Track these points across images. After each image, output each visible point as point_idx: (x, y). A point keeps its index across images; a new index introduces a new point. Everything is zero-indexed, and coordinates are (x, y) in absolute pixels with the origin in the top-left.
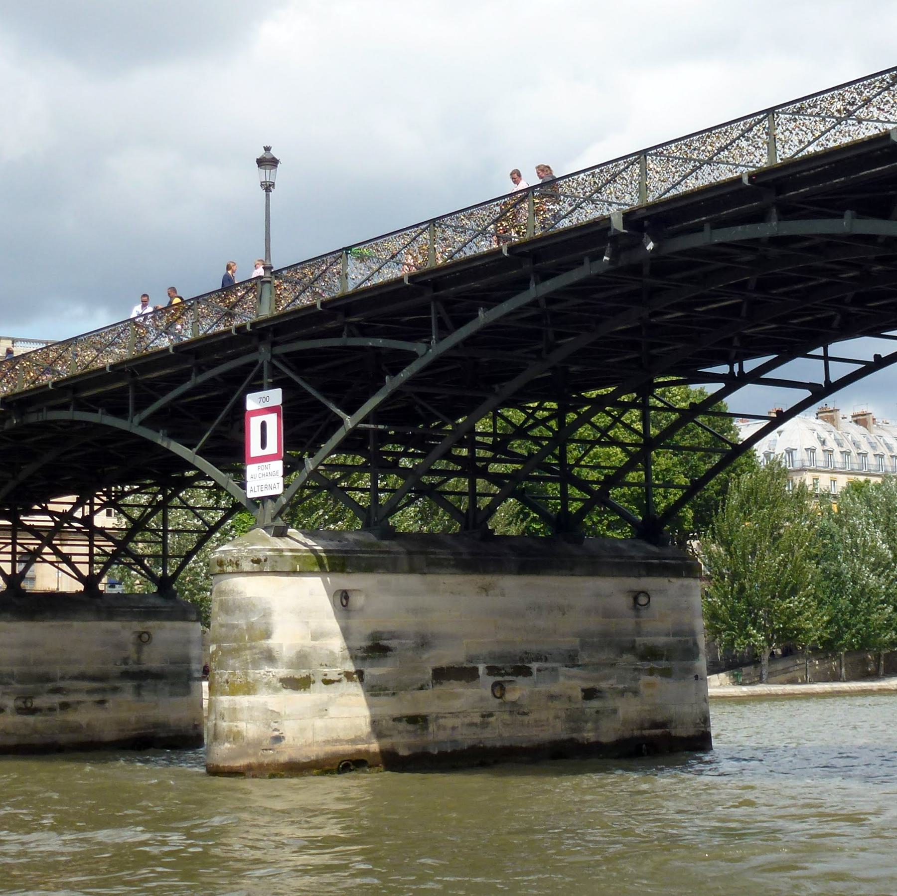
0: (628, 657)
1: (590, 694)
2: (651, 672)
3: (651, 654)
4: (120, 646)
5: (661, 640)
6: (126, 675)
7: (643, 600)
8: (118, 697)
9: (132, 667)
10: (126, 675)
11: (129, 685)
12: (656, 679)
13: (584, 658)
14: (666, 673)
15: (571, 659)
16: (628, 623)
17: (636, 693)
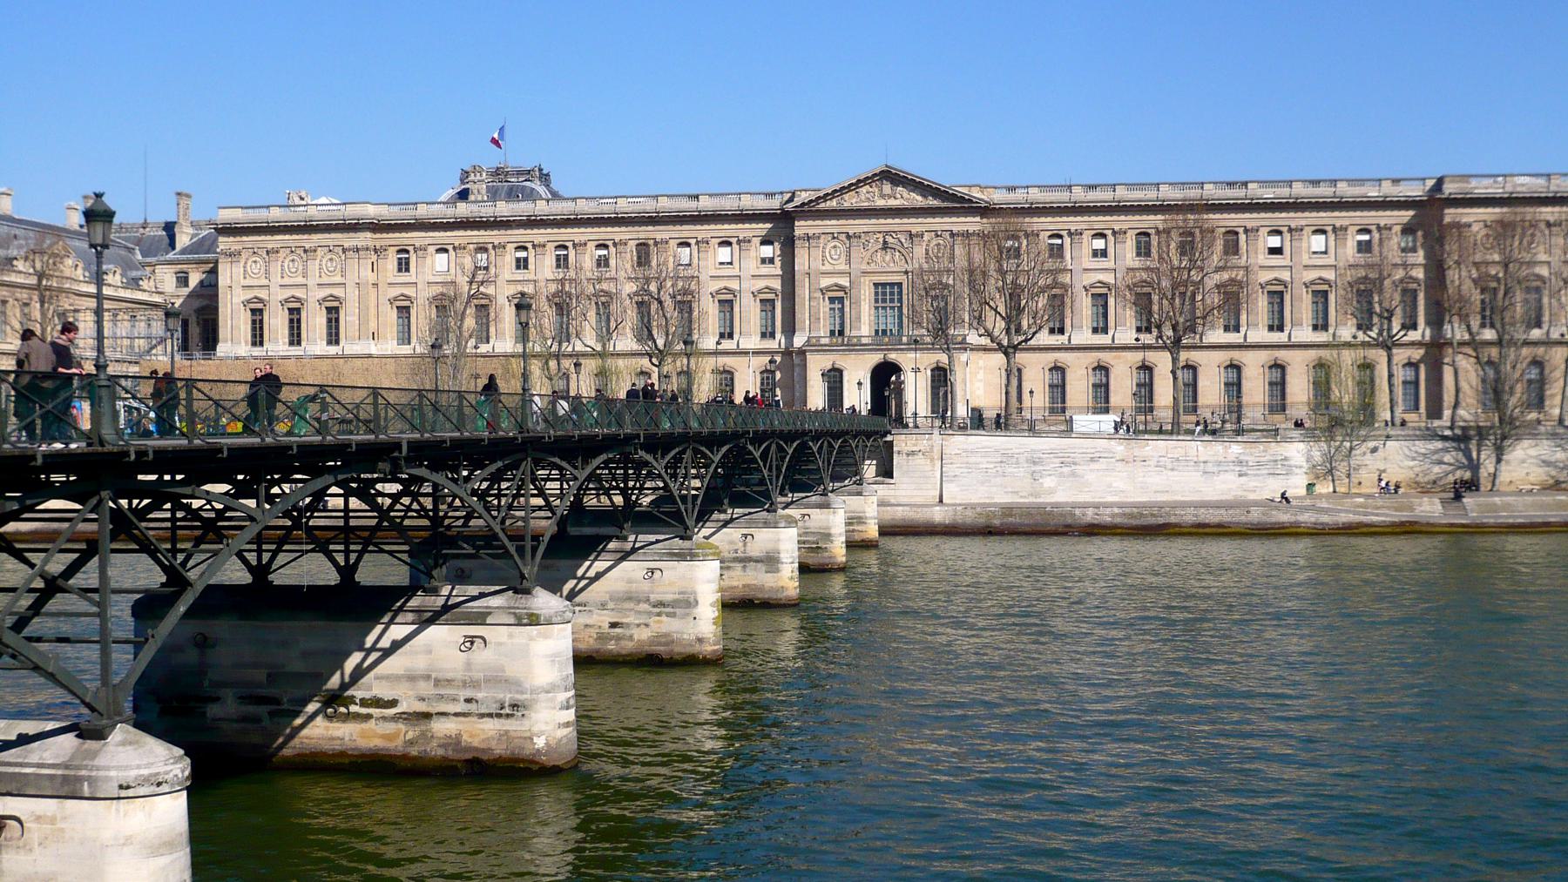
0: (644, 607)
1: (614, 625)
2: (659, 614)
3: (661, 604)
4: (731, 542)
5: (669, 597)
6: (736, 560)
7: (657, 574)
8: (731, 573)
9: (740, 554)
10: (736, 560)
11: (739, 566)
12: (664, 618)
13: (611, 605)
14: (672, 615)
15: (603, 606)
16: (646, 586)
17: (647, 625)
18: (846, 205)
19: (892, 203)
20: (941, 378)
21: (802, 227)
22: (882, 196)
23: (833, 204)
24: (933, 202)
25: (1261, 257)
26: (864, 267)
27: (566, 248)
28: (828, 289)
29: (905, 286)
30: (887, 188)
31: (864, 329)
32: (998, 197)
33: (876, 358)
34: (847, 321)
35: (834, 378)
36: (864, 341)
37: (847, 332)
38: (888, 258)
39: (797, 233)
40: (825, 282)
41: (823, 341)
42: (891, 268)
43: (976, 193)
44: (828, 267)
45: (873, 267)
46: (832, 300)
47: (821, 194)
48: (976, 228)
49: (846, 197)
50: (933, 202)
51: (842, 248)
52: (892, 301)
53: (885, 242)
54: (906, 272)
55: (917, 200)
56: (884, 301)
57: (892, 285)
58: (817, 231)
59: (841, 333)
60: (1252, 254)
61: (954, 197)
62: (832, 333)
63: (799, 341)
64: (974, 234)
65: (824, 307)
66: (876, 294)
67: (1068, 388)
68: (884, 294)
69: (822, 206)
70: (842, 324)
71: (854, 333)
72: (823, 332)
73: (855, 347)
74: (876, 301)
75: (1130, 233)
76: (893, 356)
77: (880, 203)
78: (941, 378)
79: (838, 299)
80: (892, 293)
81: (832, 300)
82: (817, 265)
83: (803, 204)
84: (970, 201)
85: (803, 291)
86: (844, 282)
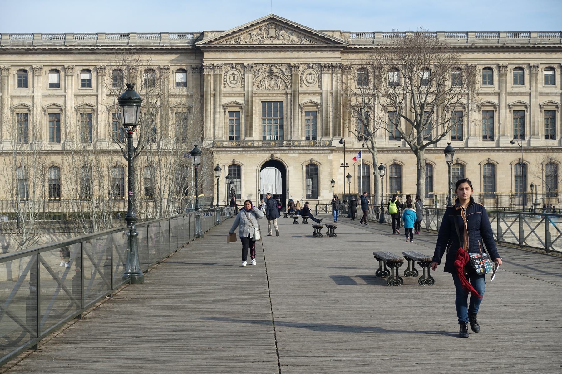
18: (242, 43)
19: (276, 42)
20: (312, 171)
21: (209, 58)
22: (269, 37)
23: (233, 42)
24: (307, 42)
25: (540, 86)
26: (255, 89)
27: (26, 71)
28: (228, 105)
29: (285, 104)
30: (272, 32)
31: (256, 136)
32: (352, 39)
33: (266, 157)
34: (242, 129)
35: (235, 171)
36: (256, 144)
37: (242, 137)
38: (273, 83)
39: (206, 63)
40: (226, 100)
41: (225, 144)
42: (275, 92)
43: (337, 36)
44: (228, 89)
45: (261, 90)
46: (231, 113)
47: (223, 34)
48: (338, 62)
49: (242, 37)
50: (307, 42)
51: (238, 76)
52: (275, 115)
53: (271, 72)
54: (286, 94)
55: (295, 39)
56: (270, 115)
57: (275, 102)
58: (220, 62)
59: (238, 137)
60: (533, 84)
61: (322, 39)
62: (231, 138)
63: (207, 143)
64: (336, 66)
65: (225, 119)
66: (264, 109)
67: (404, 179)
68: (270, 109)
69: (224, 43)
70: (239, 130)
71: (247, 138)
72: (225, 136)
73: (248, 148)
74: (264, 115)
75: (540, 66)
76: (278, 156)
77: (267, 42)
78: (312, 171)
79: (237, 113)
80: (275, 110)
81: (231, 113)
82: (220, 87)
83: (210, 41)
84: (334, 42)
85: (209, 107)
86: (240, 100)
